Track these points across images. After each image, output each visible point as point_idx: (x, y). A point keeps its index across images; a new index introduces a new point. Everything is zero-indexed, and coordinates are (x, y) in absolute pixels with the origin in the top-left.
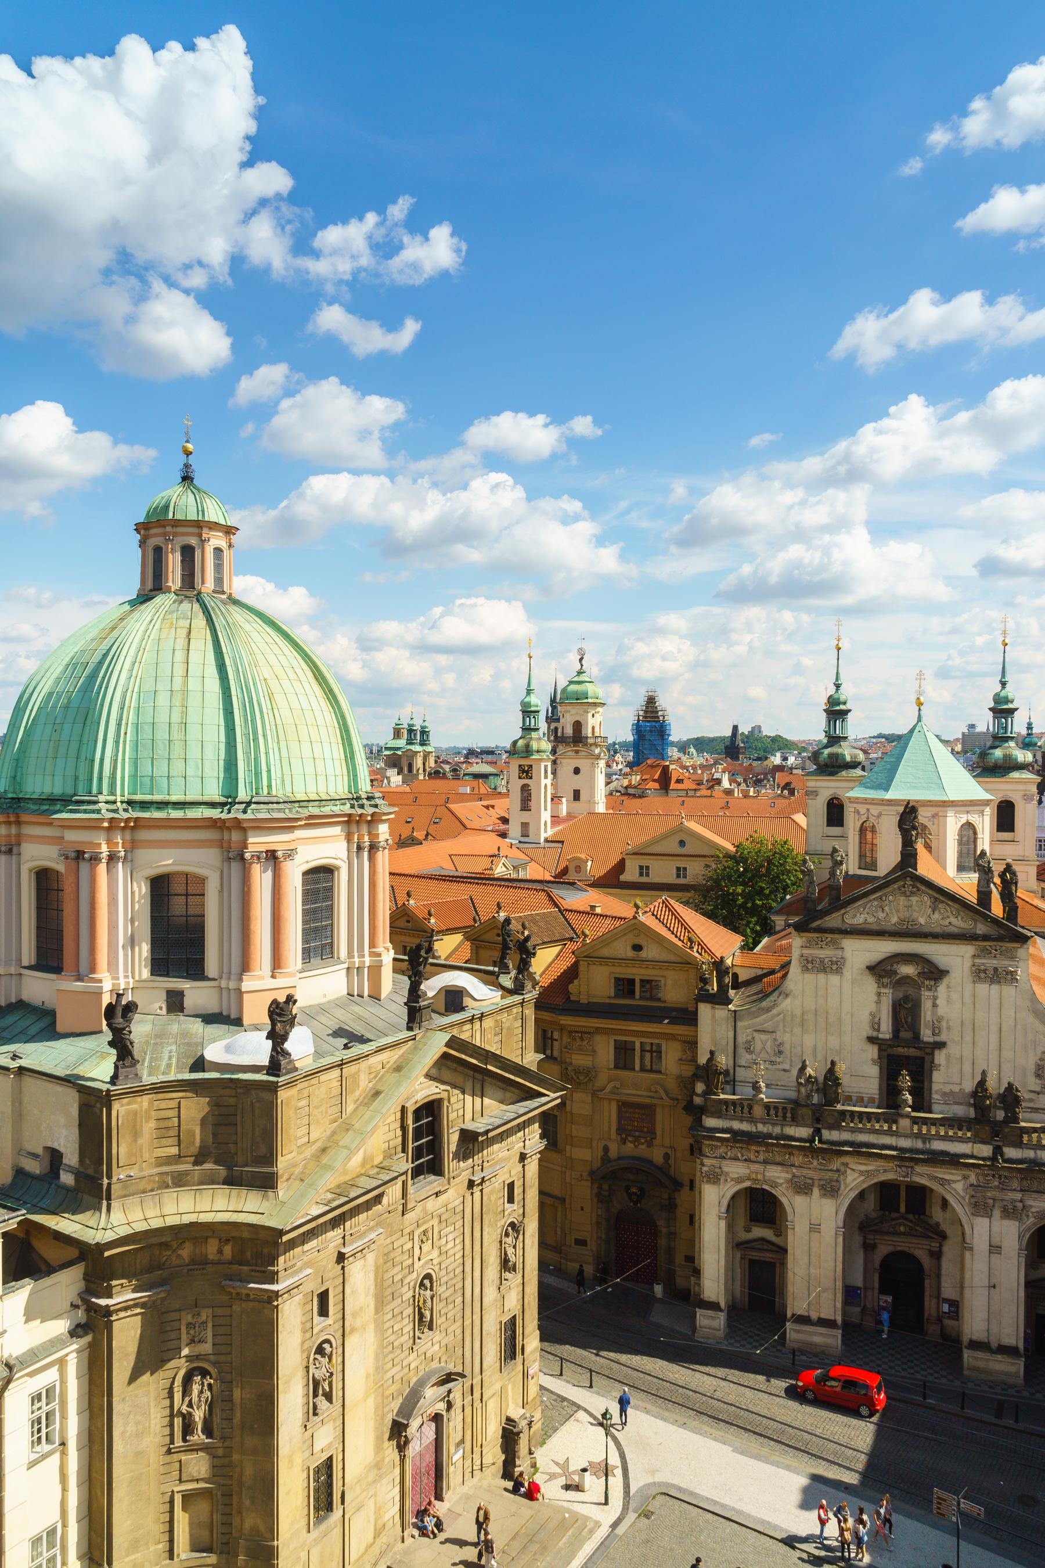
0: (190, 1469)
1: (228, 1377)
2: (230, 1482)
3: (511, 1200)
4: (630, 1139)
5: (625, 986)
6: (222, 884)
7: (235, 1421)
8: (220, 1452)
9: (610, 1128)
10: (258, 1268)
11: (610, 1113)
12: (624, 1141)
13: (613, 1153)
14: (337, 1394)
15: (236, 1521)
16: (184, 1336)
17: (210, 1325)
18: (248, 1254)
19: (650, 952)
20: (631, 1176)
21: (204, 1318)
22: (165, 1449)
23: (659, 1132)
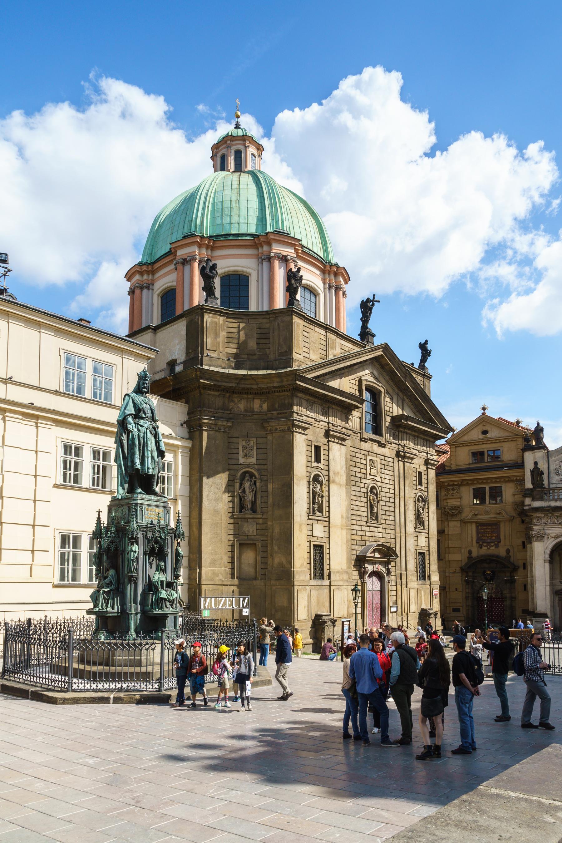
0: (244, 529)
1: (265, 478)
2: (266, 539)
3: (420, 483)
4: (485, 544)
5: (478, 455)
6: (258, 277)
7: (269, 503)
8: (261, 521)
9: (472, 540)
10: (282, 411)
11: (472, 530)
12: (481, 547)
13: (475, 554)
14: (325, 509)
15: (270, 561)
16: (241, 452)
17: (255, 448)
18: (277, 406)
19: (494, 433)
20: (486, 565)
21: (252, 444)
22: (230, 515)
23: (502, 537)
